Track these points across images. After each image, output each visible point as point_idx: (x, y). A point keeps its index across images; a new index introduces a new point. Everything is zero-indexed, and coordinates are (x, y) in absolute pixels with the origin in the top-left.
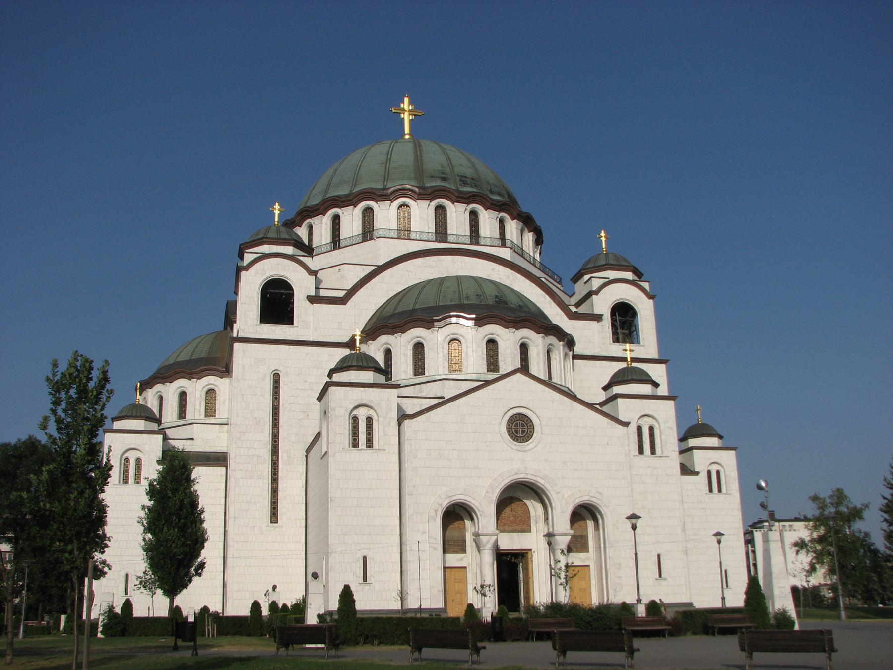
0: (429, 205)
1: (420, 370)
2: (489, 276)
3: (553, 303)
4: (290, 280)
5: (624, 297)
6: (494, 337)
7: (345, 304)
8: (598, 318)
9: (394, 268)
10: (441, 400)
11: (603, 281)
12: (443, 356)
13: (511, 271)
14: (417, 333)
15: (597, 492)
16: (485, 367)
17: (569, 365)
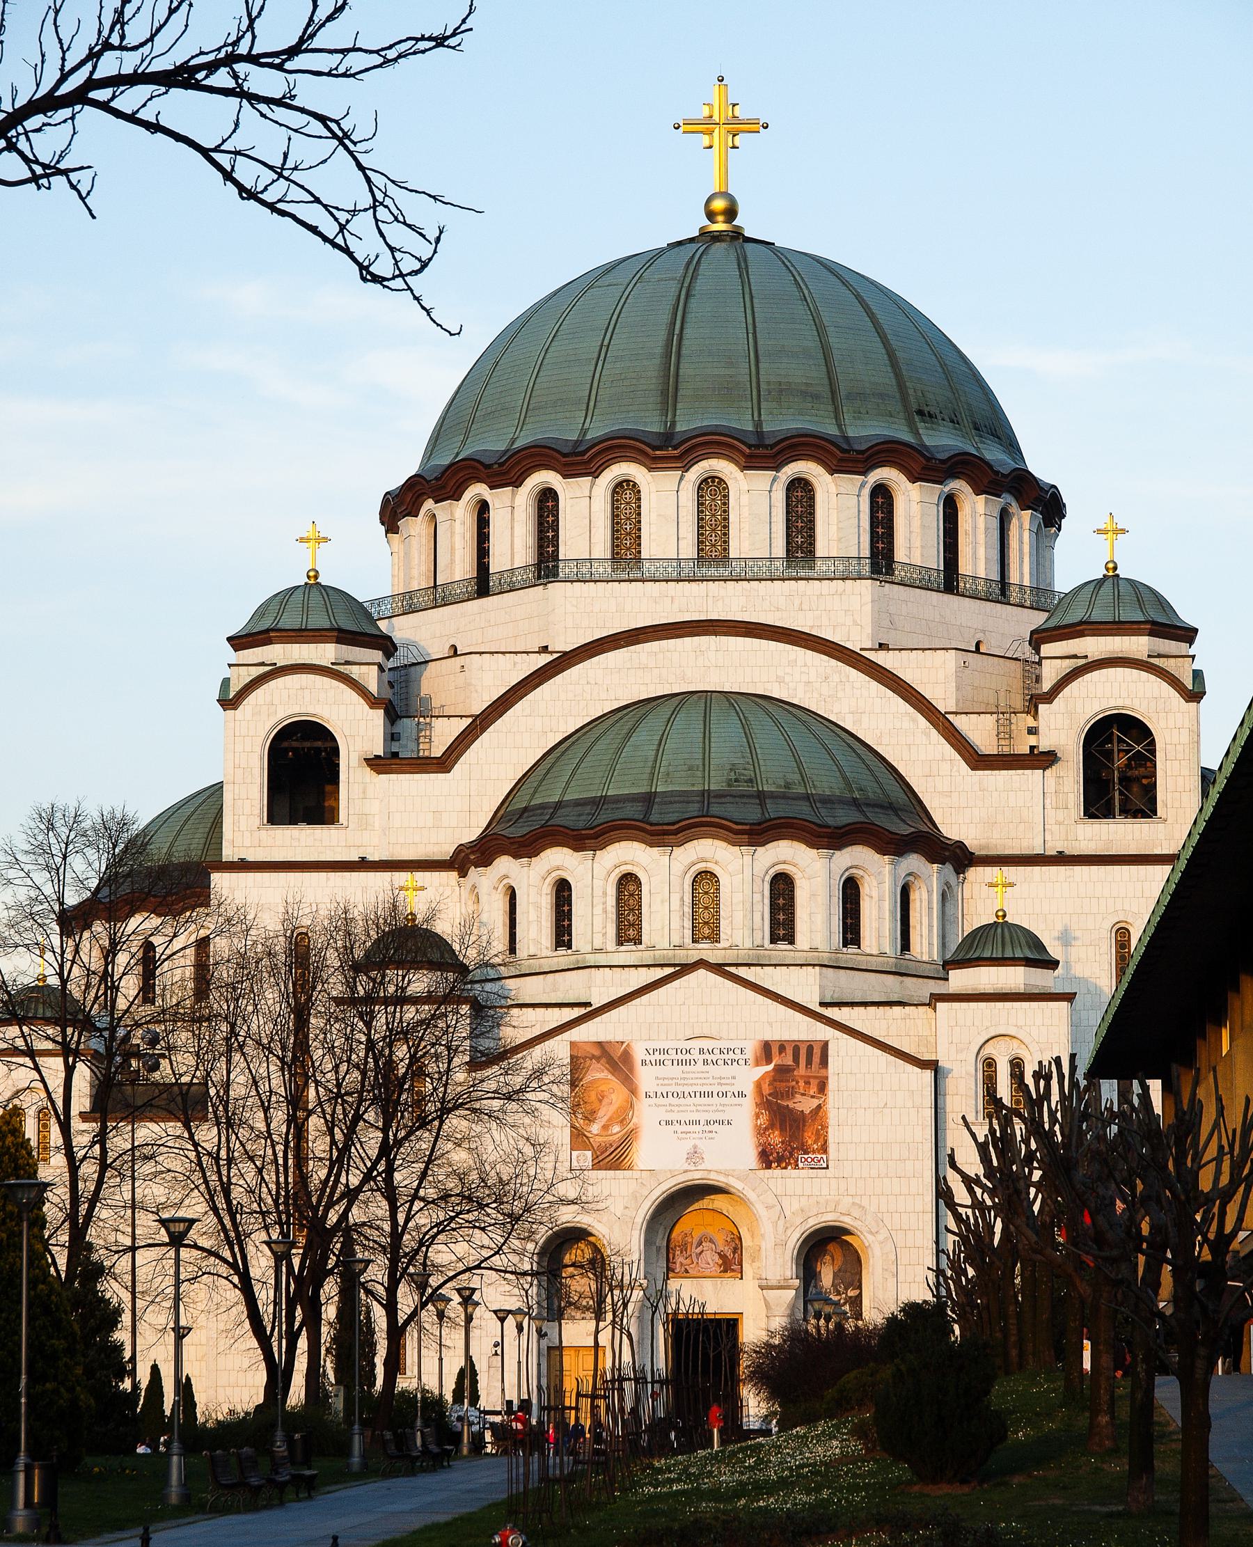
0: (681, 478)
1: (566, 938)
2: (780, 681)
3: (934, 732)
4: (328, 722)
5: (1120, 703)
6: (711, 867)
7: (449, 772)
8: (1043, 759)
9: (559, 679)
10: (582, 1011)
11: (1068, 665)
12: (605, 911)
13: (833, 662)
14: (558, 859)
15: (853, 1203)
16: (688, 933)
17: (925, 896)
